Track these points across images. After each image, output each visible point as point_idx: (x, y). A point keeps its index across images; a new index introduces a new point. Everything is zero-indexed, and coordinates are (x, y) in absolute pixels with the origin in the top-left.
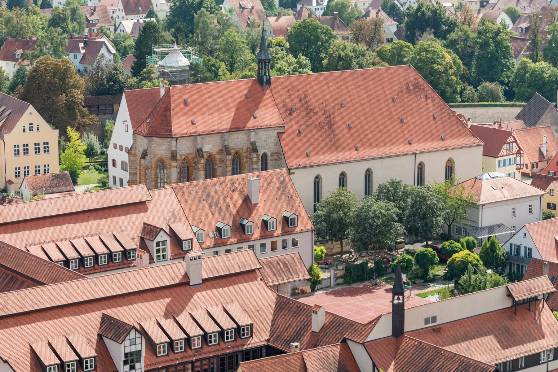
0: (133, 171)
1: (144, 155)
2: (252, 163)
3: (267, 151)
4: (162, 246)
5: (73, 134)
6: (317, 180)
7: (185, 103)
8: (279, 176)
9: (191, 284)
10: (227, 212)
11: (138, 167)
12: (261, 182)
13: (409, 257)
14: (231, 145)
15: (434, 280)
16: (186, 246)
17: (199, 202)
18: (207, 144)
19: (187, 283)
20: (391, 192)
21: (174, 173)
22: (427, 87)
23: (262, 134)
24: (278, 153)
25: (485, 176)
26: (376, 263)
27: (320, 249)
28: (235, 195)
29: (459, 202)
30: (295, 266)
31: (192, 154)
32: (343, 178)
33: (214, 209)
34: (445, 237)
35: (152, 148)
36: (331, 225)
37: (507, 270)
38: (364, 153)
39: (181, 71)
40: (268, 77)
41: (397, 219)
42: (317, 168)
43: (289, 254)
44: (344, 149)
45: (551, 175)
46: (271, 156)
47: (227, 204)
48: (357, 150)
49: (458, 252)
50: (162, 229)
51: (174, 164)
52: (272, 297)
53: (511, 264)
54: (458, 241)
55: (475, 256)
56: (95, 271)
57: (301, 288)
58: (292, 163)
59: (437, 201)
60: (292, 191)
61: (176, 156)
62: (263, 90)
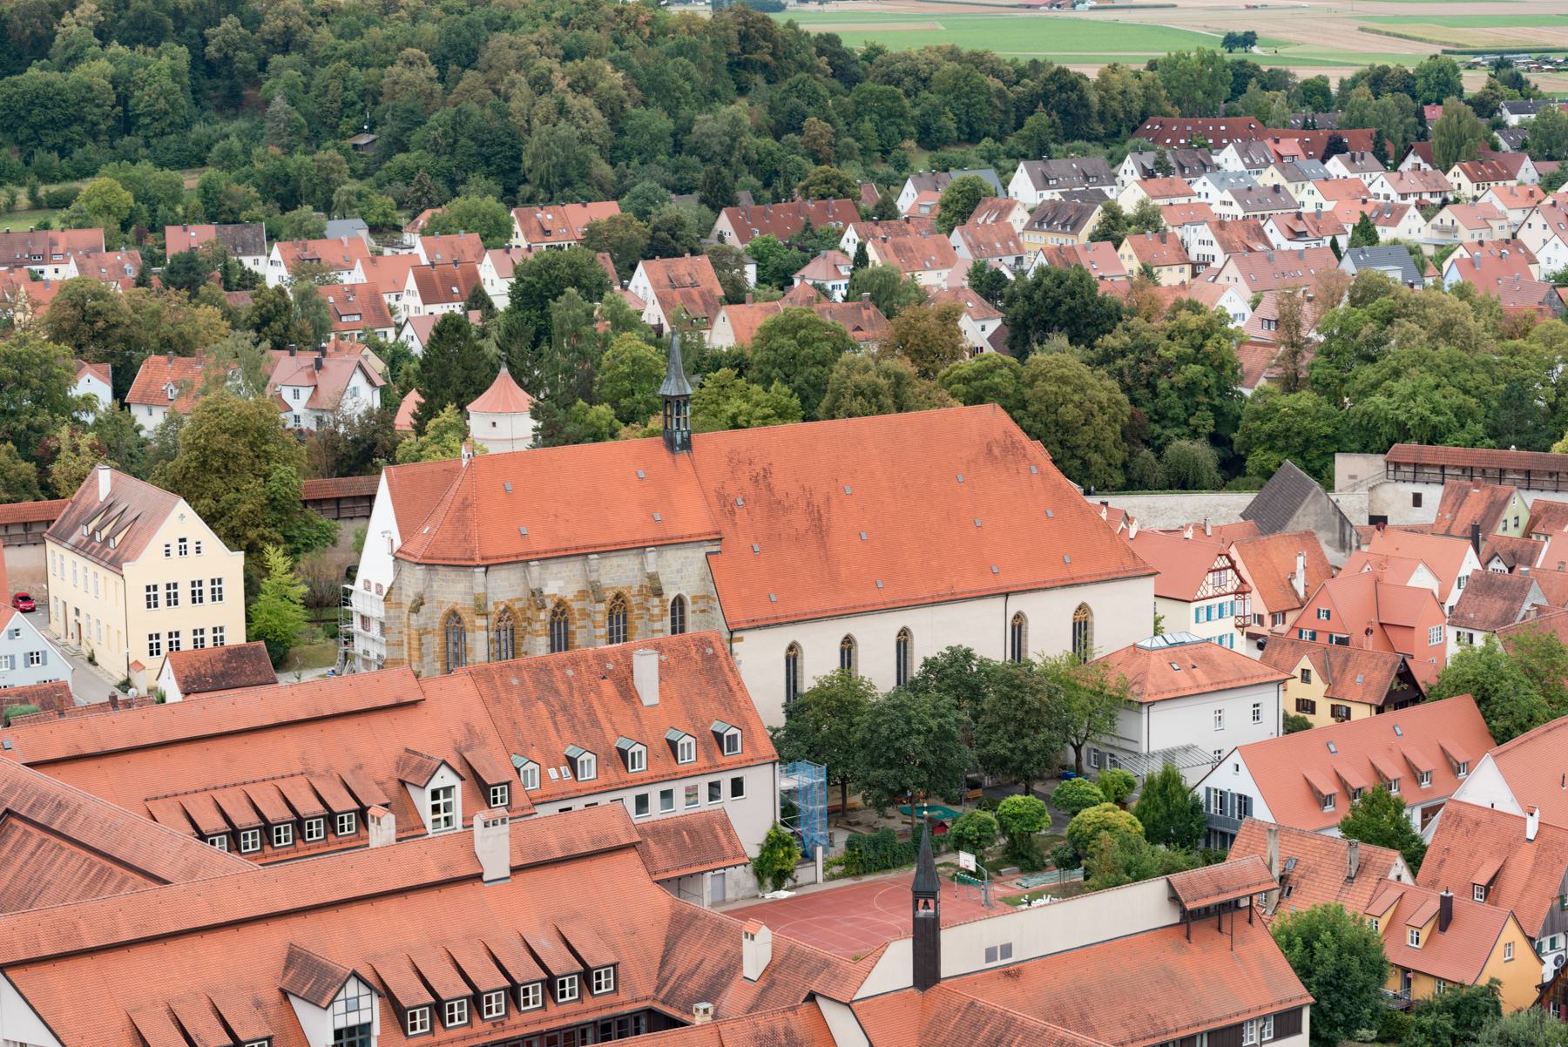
0: (394, 638)
1: (417, 607)
3: (683, 593)
11: (405, 630)
51: (481, 622)
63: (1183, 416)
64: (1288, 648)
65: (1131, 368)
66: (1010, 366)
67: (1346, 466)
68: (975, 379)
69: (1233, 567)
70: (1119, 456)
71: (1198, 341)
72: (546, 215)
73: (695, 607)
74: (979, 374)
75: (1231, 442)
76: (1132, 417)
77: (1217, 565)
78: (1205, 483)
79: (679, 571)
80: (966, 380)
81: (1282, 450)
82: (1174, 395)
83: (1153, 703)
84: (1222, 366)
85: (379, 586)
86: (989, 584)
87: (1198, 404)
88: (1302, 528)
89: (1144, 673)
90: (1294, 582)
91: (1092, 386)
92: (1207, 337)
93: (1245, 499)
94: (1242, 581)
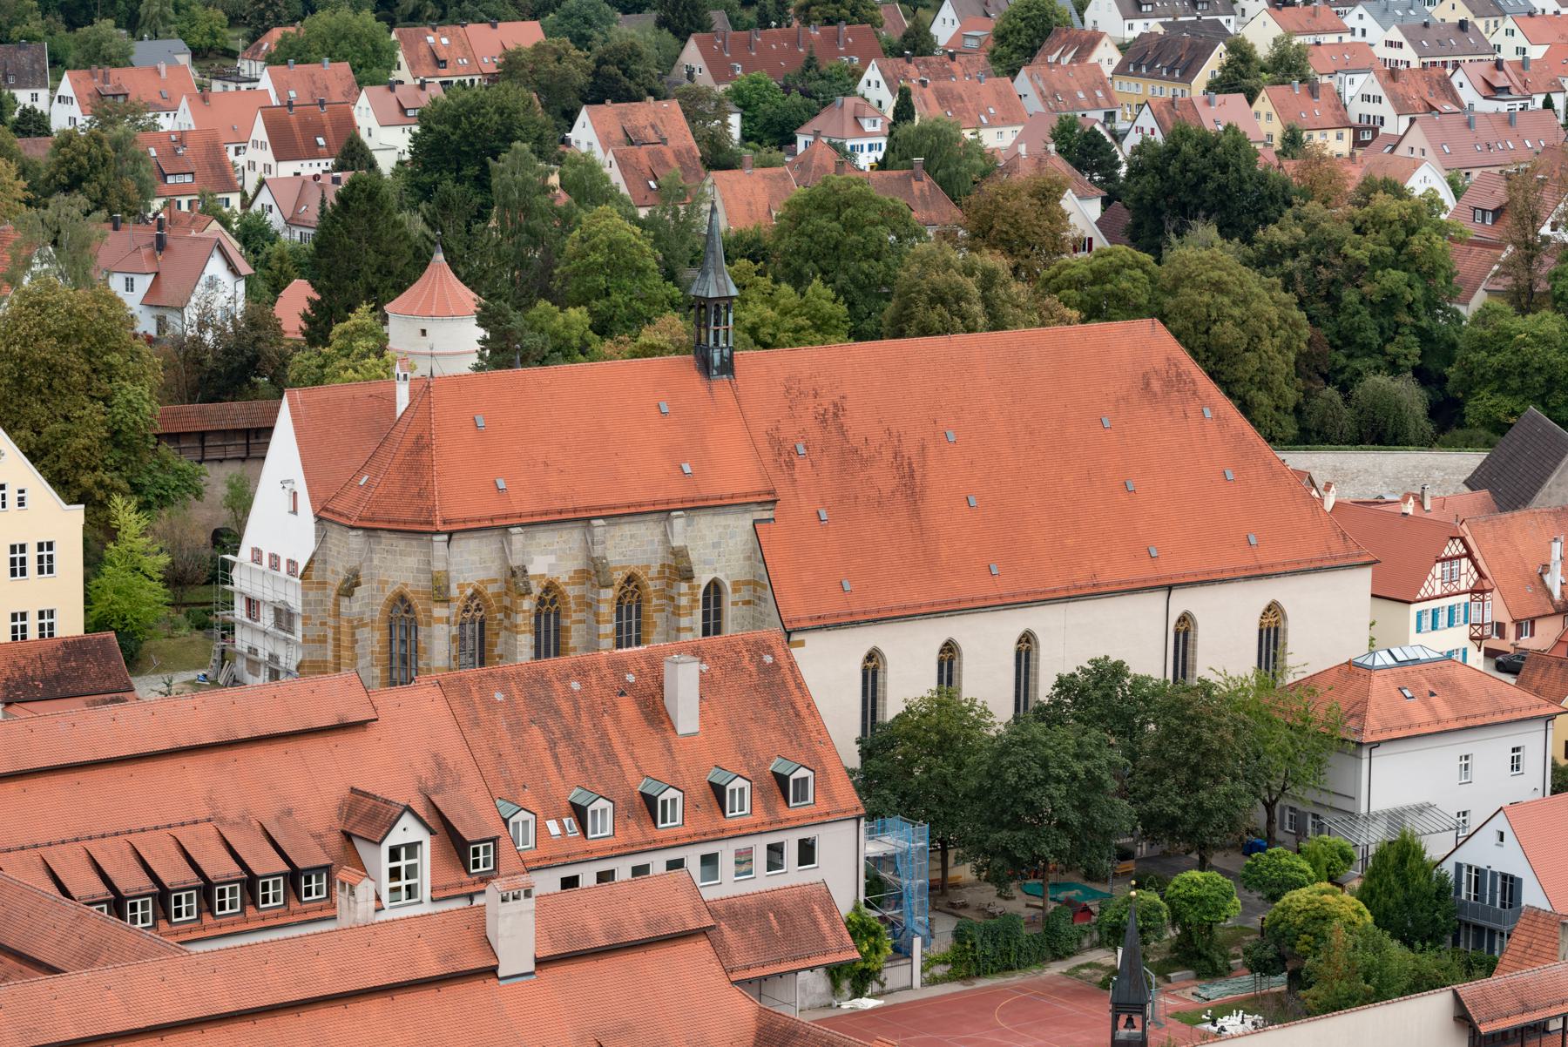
0: (315, 631)
2: (677, 611)
3: (721, 576)
4: (407, 858)
5: (124, 512)
6: (870, 665)
10: (601, 760)
11: (331, 621)
18: (542, 553)
31: (495, 581)
33: (561, 748)
35: (376, 562)
40: (726, 352)
46: (735, 591)
47: (605, 734)
50: (408, 809)
51: (440, 611)
56: (202, 934)
61: (448, 587)
62: (710, 390)
63: (1377, 341)
64: (1554, 668)
65: (1304, 271)
66: (1142, 266)
68: (1092, 283)
69: (1469, 555)
70: (1292, 396)
71: (1401, 236)
72: (439, 39)
73: (737, 597)
74: (1099, 277)
75: (1446, 379)
76: (1310, 342)
77: (1447, 552)
78: (1411, 436)
79: (715, 545)
80: (1078, 284)
81: (1515, 393)
82: (1365, 312)
83: (1378, 744)
84: (1431, 275)
85: (292, 563)
86: (1145, 572)
87: (1398, 325)
88: (1555, 502)
89: (1365, 702)
90: (1547, 578)
91: (1258, 296)
92: (1412, 231)
93: (1471, 460)
94: (1481, 575)
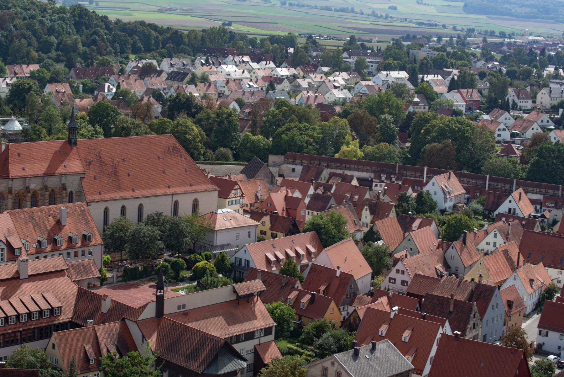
7: (19, 155)
8: (80, 207)
9: (21, 278)
12: (68, 210)
13: (167, 264)
14: (49, 185)
15: (183, 280)
16: (17, 252)
17: (26, 223)
19: (18, 278)
20: (156, 220)
21: (10, 203)
22: (182, 149)
23: (70, 179)
24: (80, 192)
25: (219, 211)
26: (144, 268)
27: (107, 257)
28: (51, 219)
29: (201, 228)
30: (91, 268)
32: (123, 209)
33: (36, 228)
34: (191, 252)
36: (115, 240)
37: (233, 275)
38: (137, 193)
39: (16, 133)
41: (159, 238)
42: (106, 202)
43: (86, 260)
44: (125, 190)
45: (264, 211)
48: (133, 190)
49: (199, 262)
51: (10, 196)
52: (74, 289)
53: (235, 271)
54: (200, 254)
55: (211, 265)
57: (93, 283)
58: (90, 198)
59: (187, 227)
60: (89, 217)
67: (272, 158)
69: (240, 188)
77: (235, 188)
94: (243, 193)
